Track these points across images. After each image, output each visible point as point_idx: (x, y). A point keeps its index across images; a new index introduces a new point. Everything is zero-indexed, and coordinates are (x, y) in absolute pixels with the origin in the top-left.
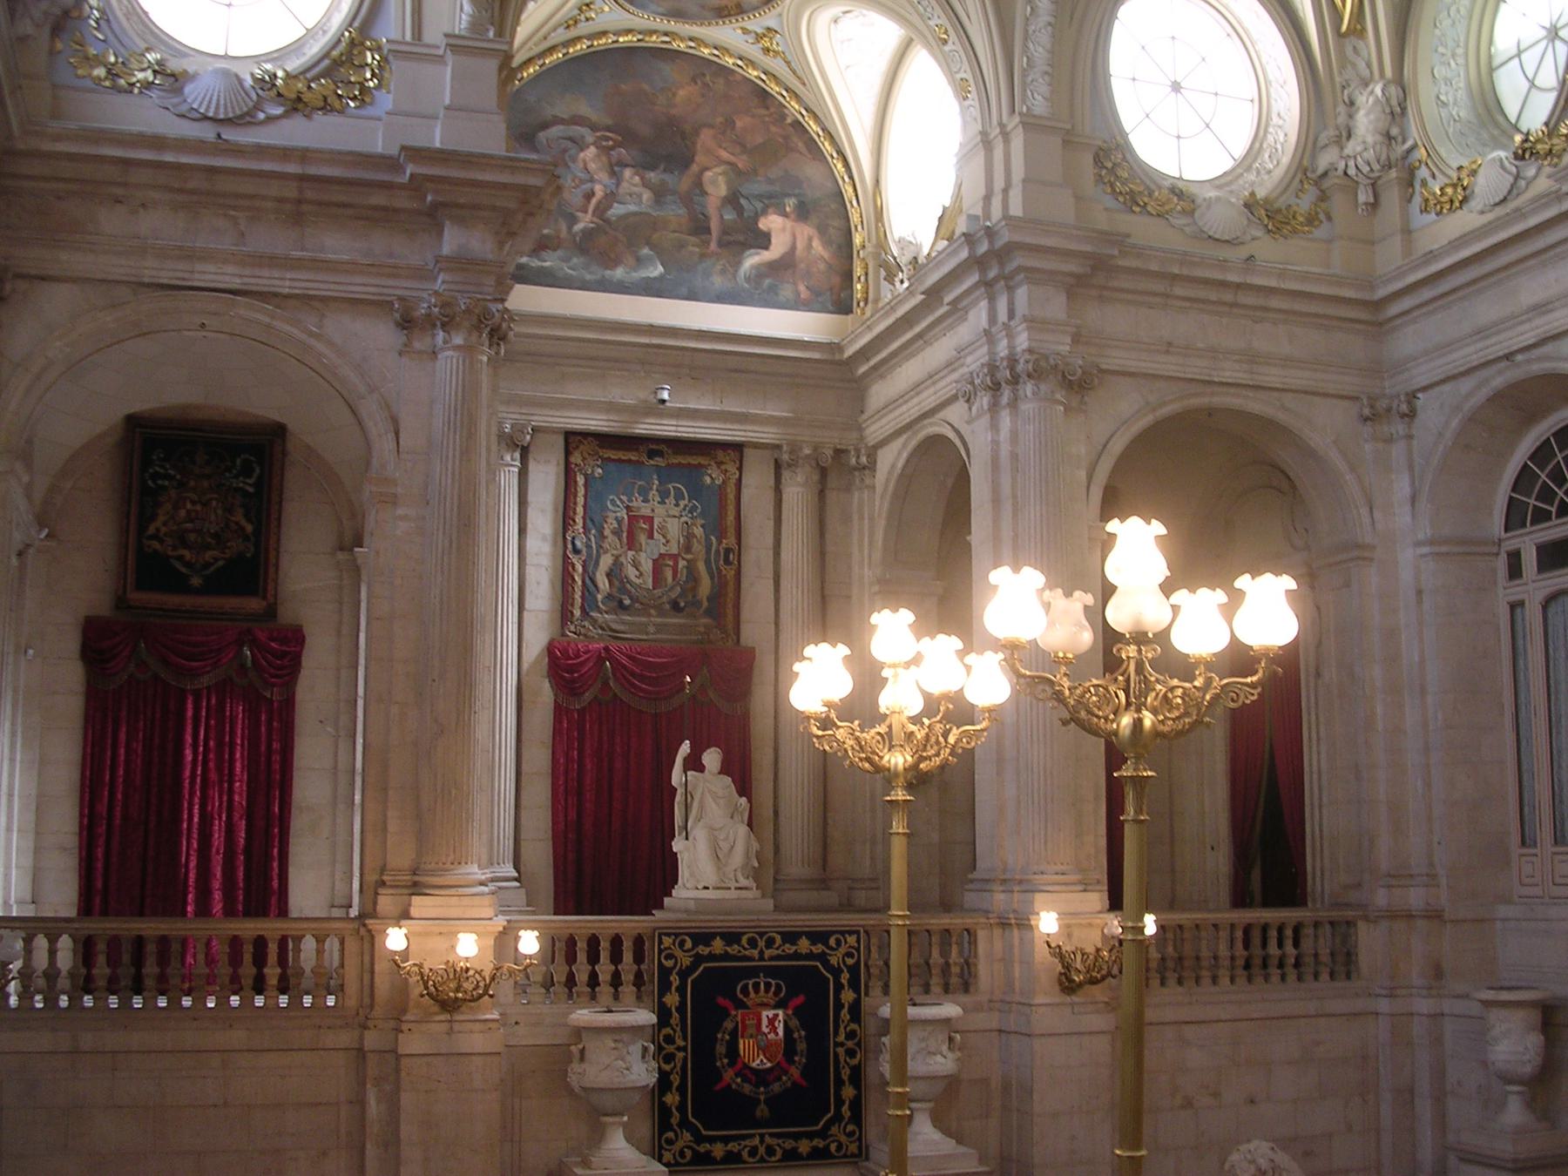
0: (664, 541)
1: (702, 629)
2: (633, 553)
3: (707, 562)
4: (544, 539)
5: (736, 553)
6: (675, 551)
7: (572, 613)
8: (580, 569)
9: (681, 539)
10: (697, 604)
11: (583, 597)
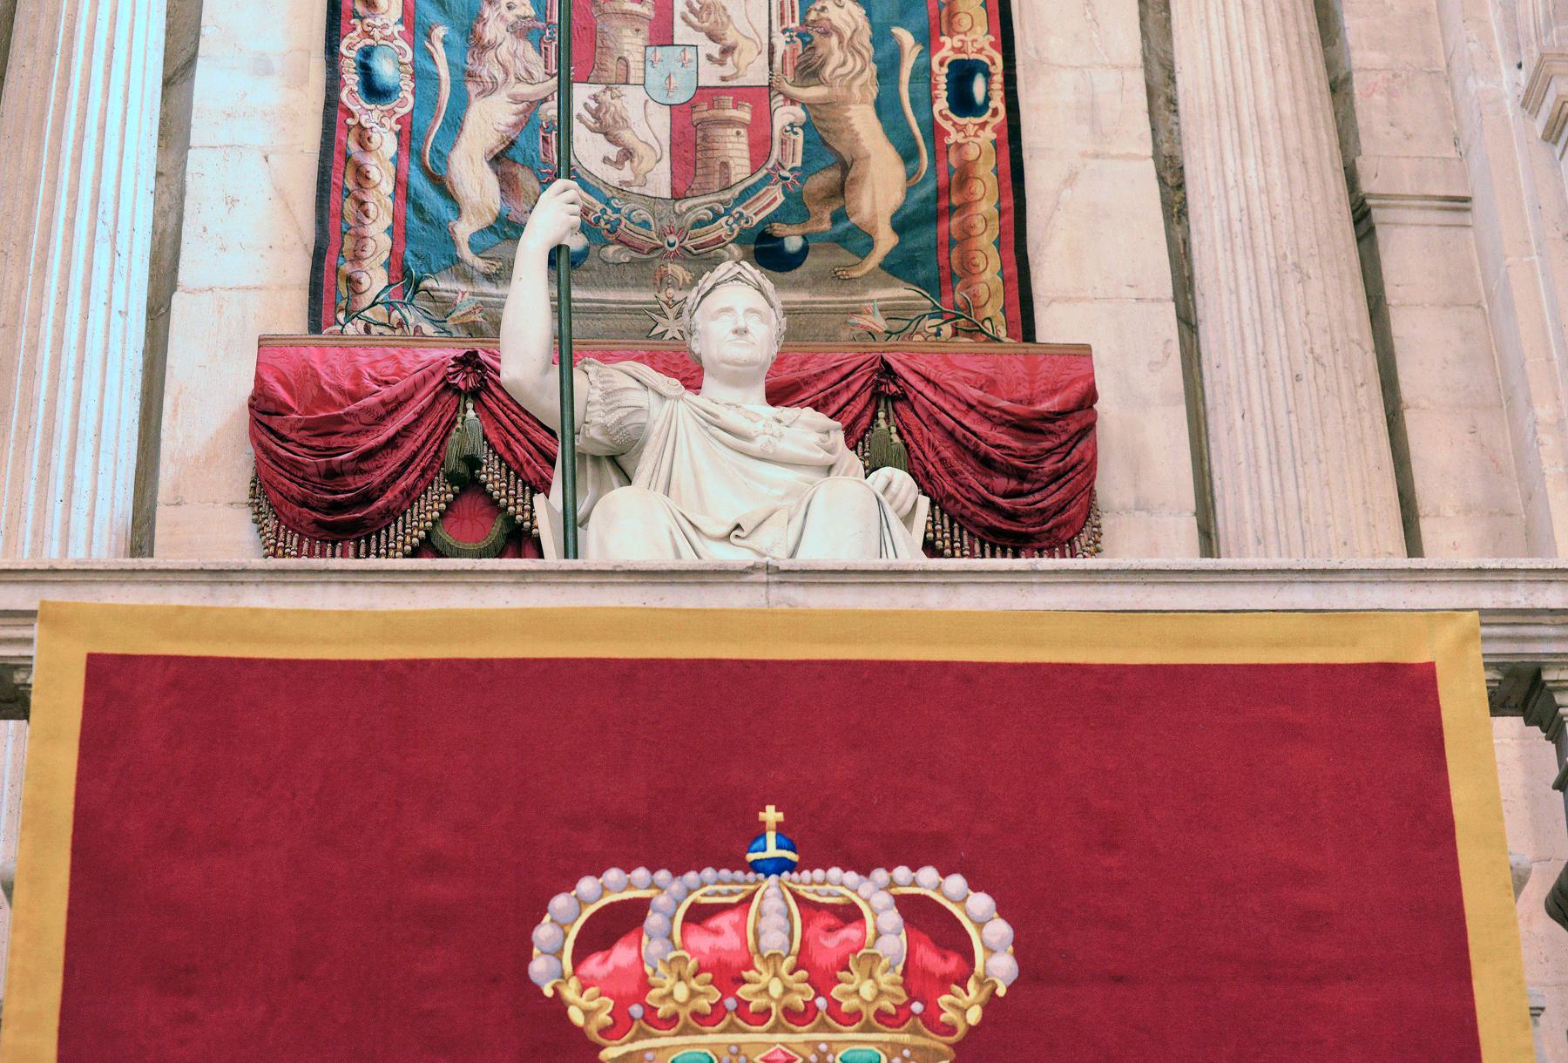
0: (715, 49)
1: (879, 323)
2: (596, 89)
3: (886, 108)
4: (263, 67)
5: (998, 78)
6: (755, 73)
7: (352, 282)
8: (386, 143)
9: (780, 43)
10: (856, 240)
11: (398, 231)
